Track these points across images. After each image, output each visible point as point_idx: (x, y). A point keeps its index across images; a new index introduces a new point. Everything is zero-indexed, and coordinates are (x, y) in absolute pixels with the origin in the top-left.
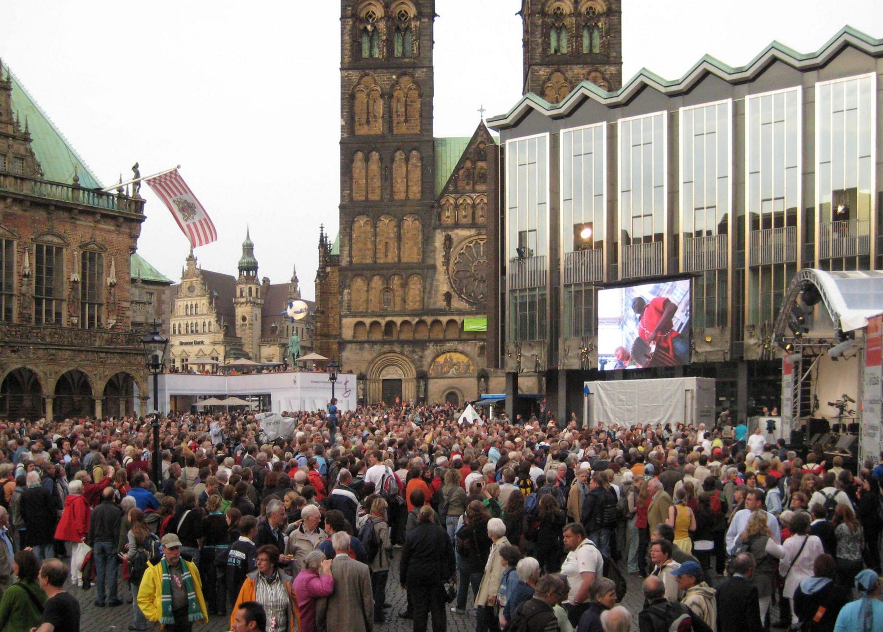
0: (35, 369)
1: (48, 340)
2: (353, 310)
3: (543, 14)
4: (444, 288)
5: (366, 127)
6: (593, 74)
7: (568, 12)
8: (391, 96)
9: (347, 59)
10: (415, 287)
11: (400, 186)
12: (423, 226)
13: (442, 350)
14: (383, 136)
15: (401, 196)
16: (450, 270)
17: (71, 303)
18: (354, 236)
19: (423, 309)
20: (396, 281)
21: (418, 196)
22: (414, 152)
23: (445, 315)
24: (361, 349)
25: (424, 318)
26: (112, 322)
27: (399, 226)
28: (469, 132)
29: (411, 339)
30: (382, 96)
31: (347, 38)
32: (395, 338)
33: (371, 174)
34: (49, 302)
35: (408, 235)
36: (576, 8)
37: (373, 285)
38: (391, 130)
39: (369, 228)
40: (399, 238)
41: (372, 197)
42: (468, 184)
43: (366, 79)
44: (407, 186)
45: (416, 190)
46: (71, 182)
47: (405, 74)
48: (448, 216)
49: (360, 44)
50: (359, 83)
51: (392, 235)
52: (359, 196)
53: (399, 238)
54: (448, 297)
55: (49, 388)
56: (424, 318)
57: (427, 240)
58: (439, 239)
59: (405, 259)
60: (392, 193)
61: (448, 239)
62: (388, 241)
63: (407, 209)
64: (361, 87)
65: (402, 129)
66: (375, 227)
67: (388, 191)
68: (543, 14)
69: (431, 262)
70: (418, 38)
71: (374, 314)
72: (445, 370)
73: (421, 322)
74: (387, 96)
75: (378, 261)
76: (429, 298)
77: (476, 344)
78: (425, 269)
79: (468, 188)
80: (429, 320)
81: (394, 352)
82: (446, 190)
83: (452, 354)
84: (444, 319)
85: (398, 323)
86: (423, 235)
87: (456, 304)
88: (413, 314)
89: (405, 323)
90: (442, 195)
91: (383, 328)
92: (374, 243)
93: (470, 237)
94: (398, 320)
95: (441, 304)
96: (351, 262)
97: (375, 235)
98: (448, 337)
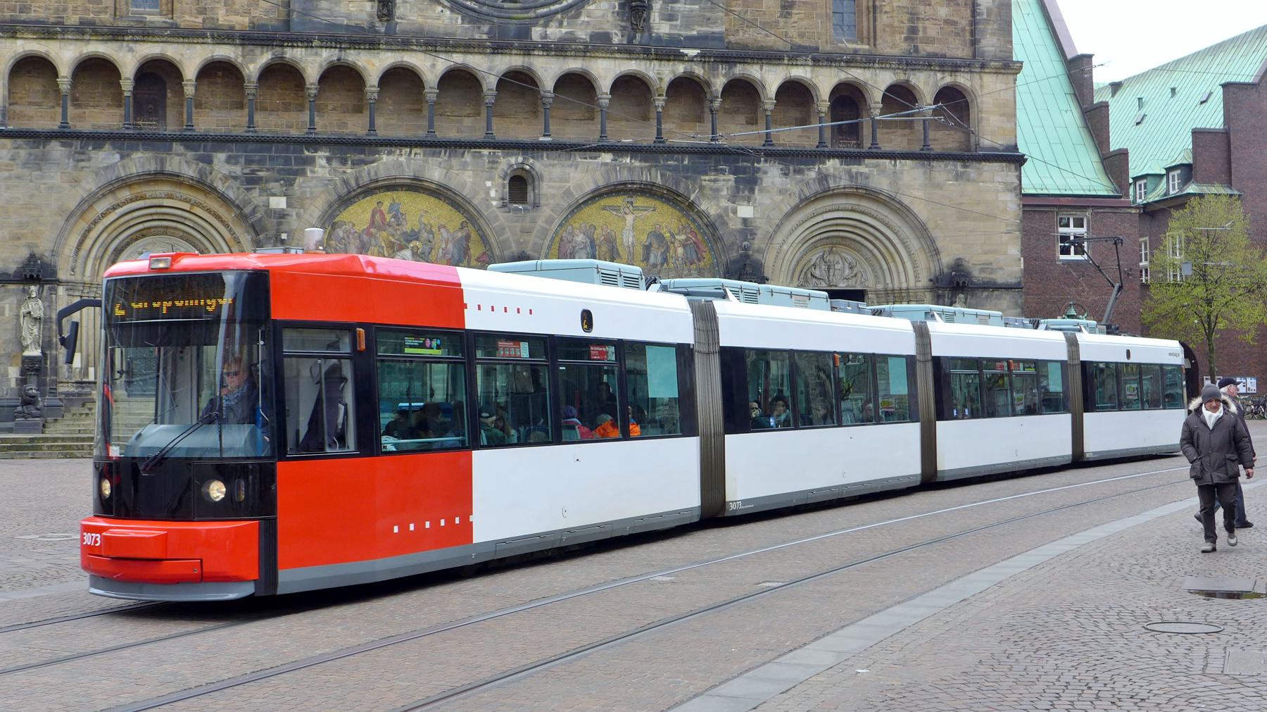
13: (365, 179)
19: (287, 23)
24: (39, 162)
25: (294, 54)
29: (240, 132)
32: (171, 128)
56: (294, 54)
71: (85, 30)
77: (493, 162)
83: (404, 198)
84: (373, 64)
85: (190, 71)
88: (252, 38)
89: (215, 71)
91: (127, 85)
94: (191, 59)
98: (382, 133)
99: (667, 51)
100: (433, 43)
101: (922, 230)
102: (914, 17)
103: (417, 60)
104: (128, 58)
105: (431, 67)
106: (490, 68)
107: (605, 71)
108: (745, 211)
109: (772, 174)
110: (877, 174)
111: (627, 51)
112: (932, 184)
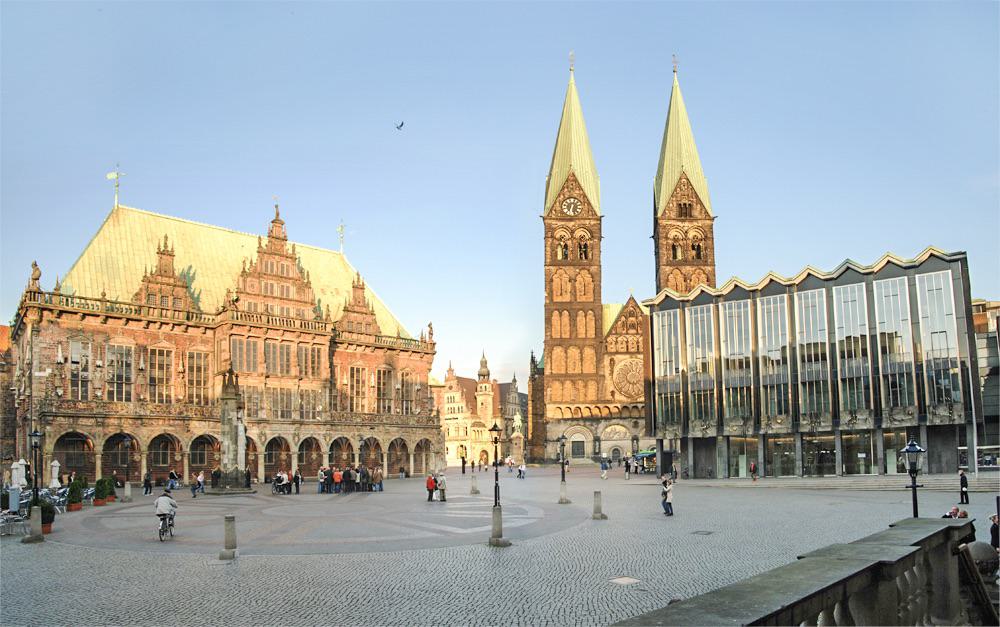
0: (378, 438)
1: (385, 421)
2: (553, 400)
9: (548, 260)
10: (592, 387)
14: (570, 302)
15: (584, 336)
17: (396, 401)
18: (554, 357)
20: (581, 384)
21: (593, 336)
26: (418, 410)
31: (548, 249)
34: (384, 400)
37: (566, 386)
39: (563, 354)
40: (582, 360)
41: (564, 336)
45: (592, 333)
46: (396, 335)
48: (612, 348)
49: (556, 252)
52: (556, 335)
53: (582, 360)
55: (385, 448)
57: (599, 361)
58: (607, 360)
59: (584, 372)
61: (612, 360)
63: (587, 342)
65: (581, 299)
66: (566, 352)
69: (602, 373)
71: (566, 402)
74: (572, 280)
78: (599, 378)
82: (610, 333)
87: (618, 396)
88: (592, 402)
90: (608, 336)
92: (566, 362)
95: (609, 397)
97: (567, 358)
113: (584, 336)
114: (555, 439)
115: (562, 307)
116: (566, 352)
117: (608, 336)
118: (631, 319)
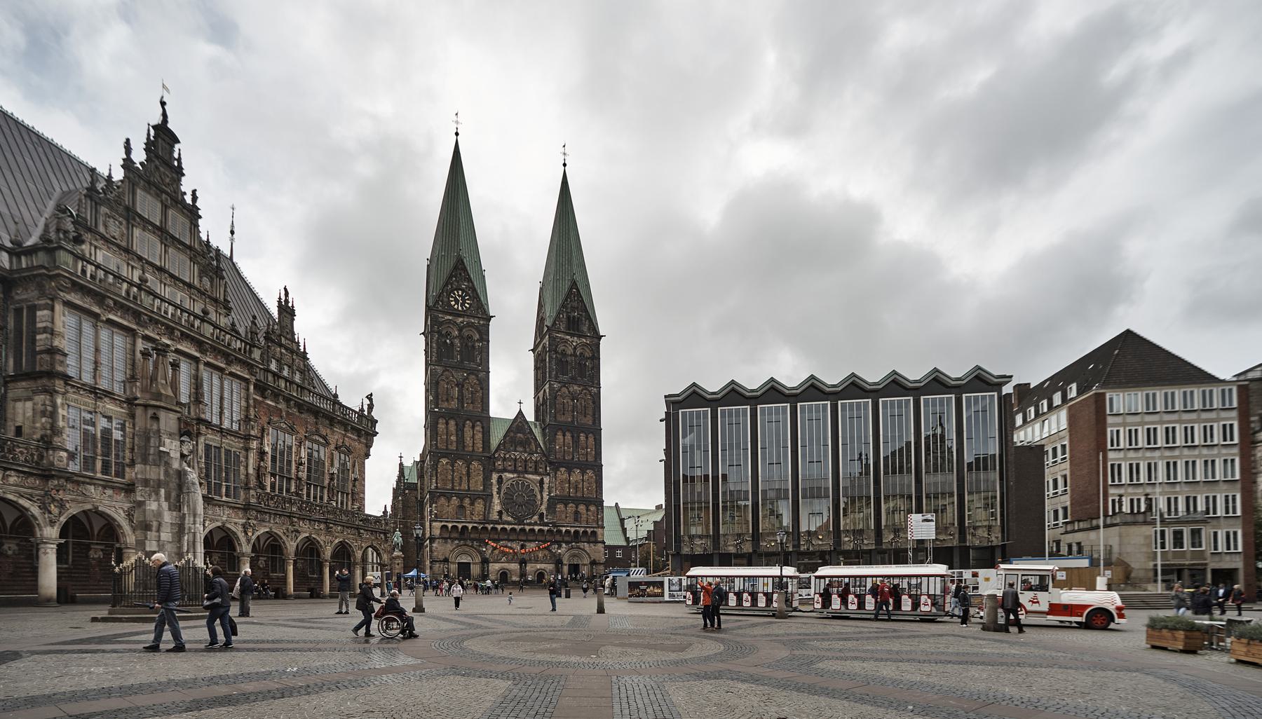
3: (556, 352)
4: (497, 508)
5: (446, 403)
6: (585, 391)
7: (570, 353)
8: (463, 386)
10: (479, 506)
11: (468, 441)
12: (484, 469)
14: (458, 410)
16: (501, 497)
20: (467, 501)
21: (481, 449)
22: (478, 423)
23: (499, 524)
24: (446, 542)
25: (487, 525)
27: (468, 467)
28: (512, 415)
30: (457, 385)
33: (450, 433)
35: (474, 473)
36: (575, 352)
38: (463, 407)
40: (468, 474)
42: (512, 446)
43: (447, 373)
44: (474, 443)
45: (479, 445)
47: (473, 374)
50: (442, 375)
51: (464, 473)
53: (468, 474)
54: (500, 513)
56: (487, 525)
57: (487, 478)
58: (495, 476)
60: (464, 446)
61: (500, 478)
62: (462, 475)
63: (474, 458)
64: (444, 378)
65: (471, 407)
66: (453, 466)
67: (462, 445)
68: (556, 352)
70: (481, 353)
72: (499, 558)
73: (485, 529)
75: (455, 488)
76: (489, 513)
78: (488, 498)
79: (512, 448)
80: (490, 527)
81: (468, 545)
84: (499, 527)
86: (484, 474)
87: (505, 518)
91: (460, 530)
92: (453, 475)
93: (513, 478)
94: (470, 526)
96: (437, 486)
99: (546, 524)
100: (509, 523)
101: (588, 554)
102: (587, 519)
103: (506, 526)
104: (460, 526)
105: (508, 527)
106: (518, 527)
107: (537, 528)
108: (559, 551)
109: (564, 545)
110: (581, 545)
111: (540, 525)
112: (590, 547)
113: (471, 449)
114: (442, 558)
115: (449, 415)
116: (453, 466)
117: (496, 451)
118: (519, 435)
